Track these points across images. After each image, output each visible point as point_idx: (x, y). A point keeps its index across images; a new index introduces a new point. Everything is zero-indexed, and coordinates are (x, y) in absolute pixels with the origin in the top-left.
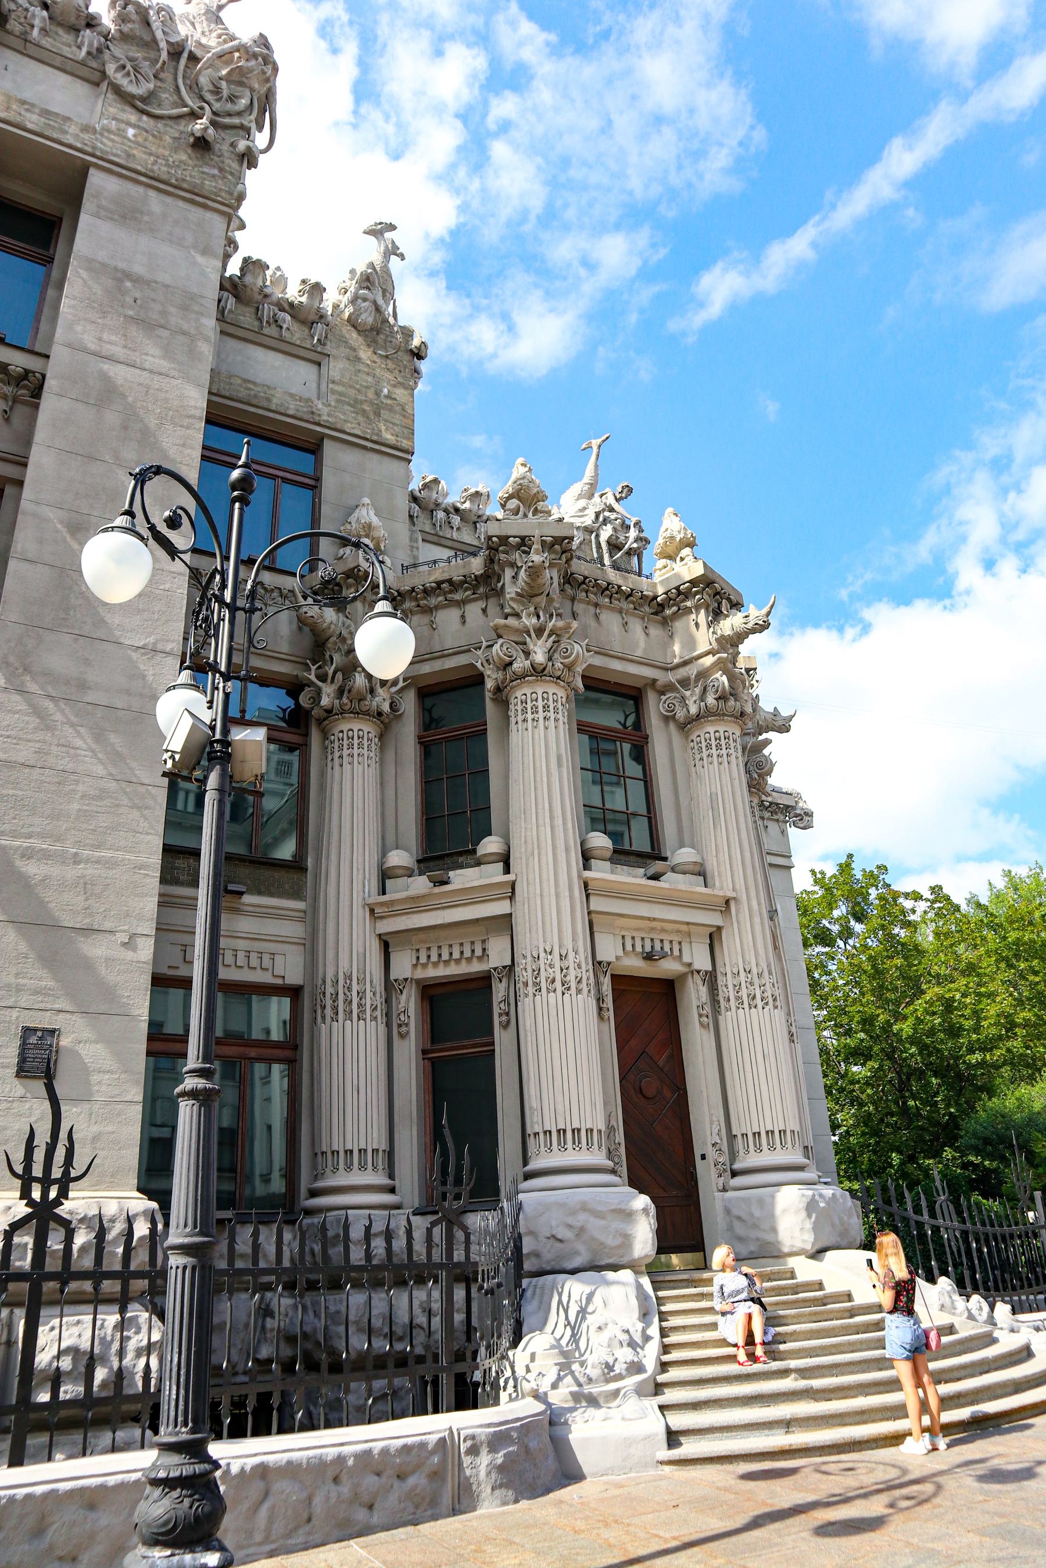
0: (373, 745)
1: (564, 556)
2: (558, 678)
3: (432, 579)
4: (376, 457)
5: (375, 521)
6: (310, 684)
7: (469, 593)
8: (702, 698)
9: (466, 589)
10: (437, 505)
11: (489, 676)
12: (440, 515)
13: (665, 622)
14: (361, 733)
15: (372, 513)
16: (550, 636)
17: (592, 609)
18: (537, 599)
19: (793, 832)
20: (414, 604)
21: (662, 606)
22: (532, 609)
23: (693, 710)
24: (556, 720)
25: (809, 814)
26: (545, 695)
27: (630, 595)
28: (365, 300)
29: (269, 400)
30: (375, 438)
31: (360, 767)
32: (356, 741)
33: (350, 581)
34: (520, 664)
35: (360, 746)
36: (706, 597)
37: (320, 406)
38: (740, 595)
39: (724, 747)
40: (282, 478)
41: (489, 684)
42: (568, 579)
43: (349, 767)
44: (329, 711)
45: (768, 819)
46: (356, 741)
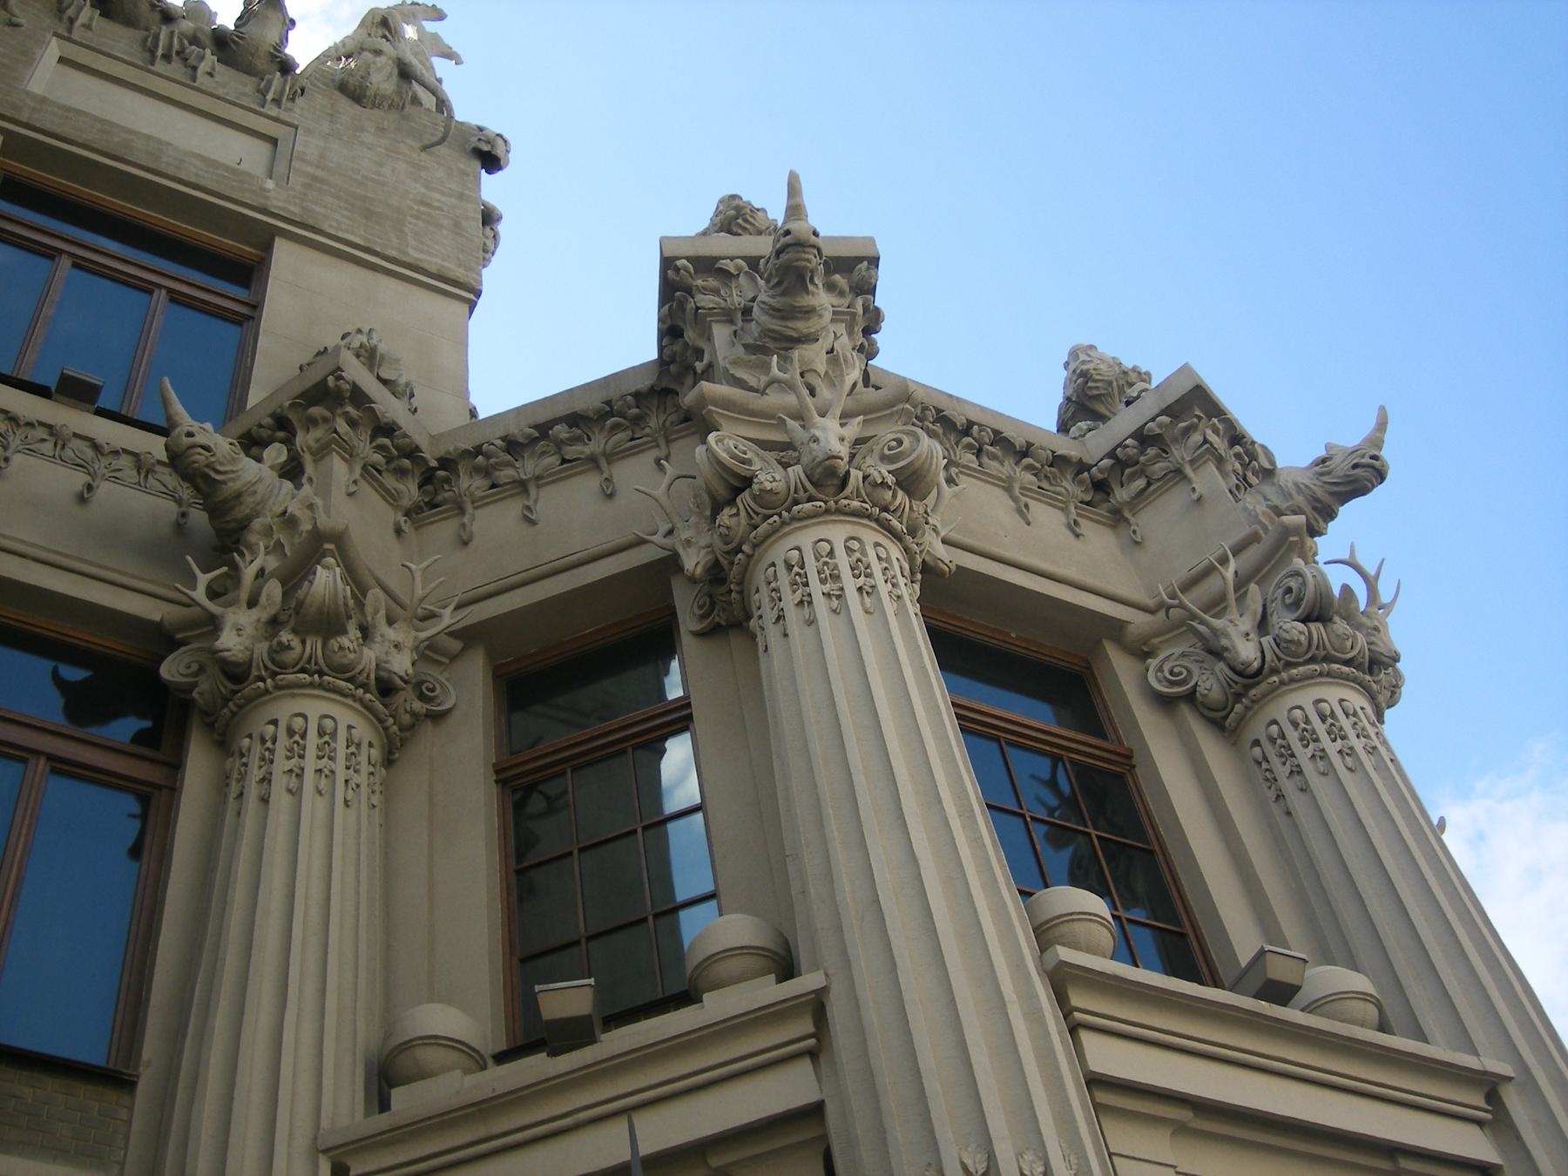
0: (363, 758)
9: (616, 428)
13: (1117, 519)
20: (479, 483)
27: (1025, 454)
28: (378, 53)
31: (321, 803)
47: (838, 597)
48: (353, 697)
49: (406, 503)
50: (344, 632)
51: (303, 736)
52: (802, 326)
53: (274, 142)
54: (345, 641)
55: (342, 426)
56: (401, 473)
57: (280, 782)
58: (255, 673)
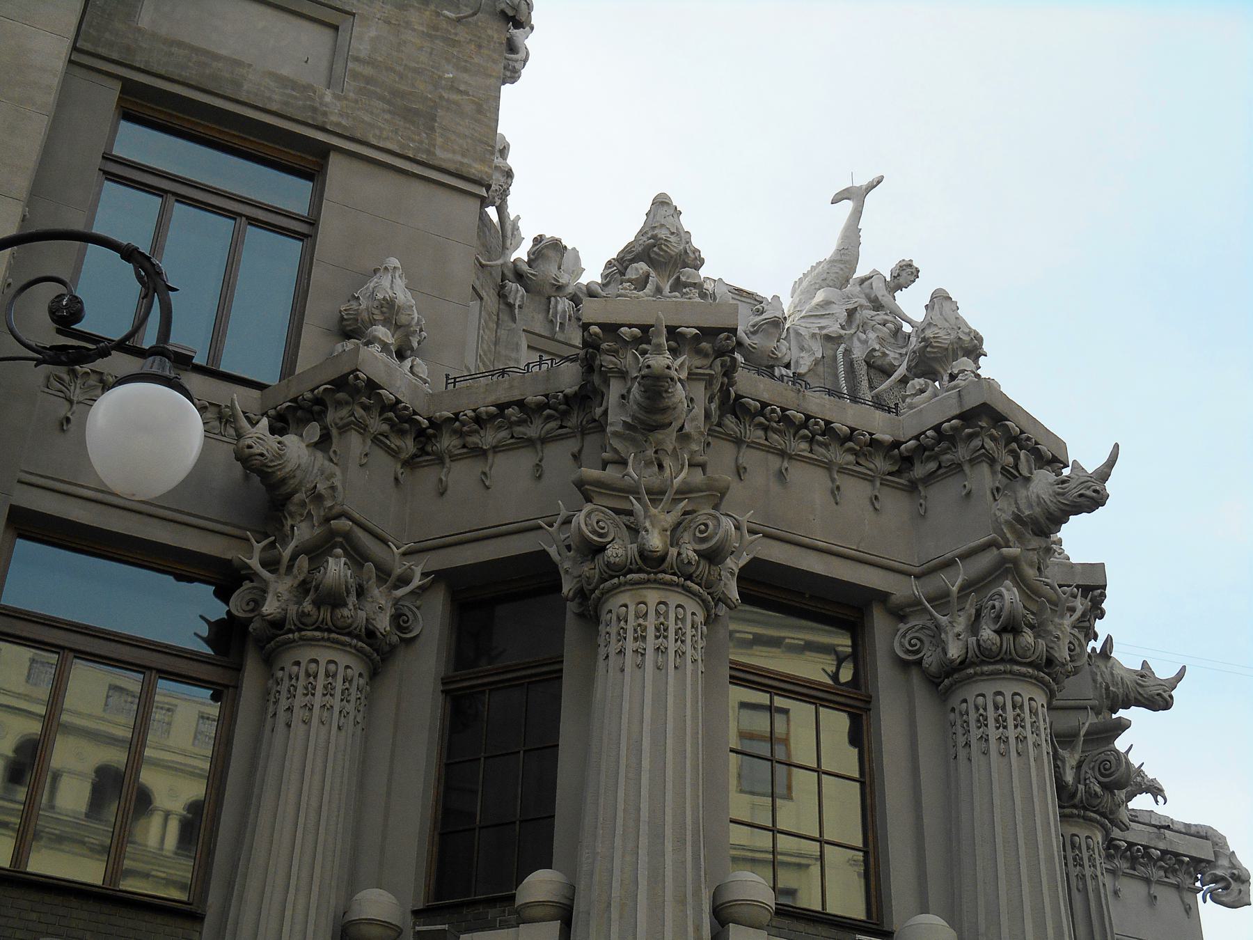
0: (353, 690)
1: (718, 362)
2: (689, 577)
3: (492, 398)
4: (419, 188)
5: (402, 295)
6: (252, 576)
7: (553, 424)
8: (974, 628)
9: (549, 418)
10: (560, 288)
11: (567, 572)
12: (564, 304)
13: (912, 488)
14: (332, 667)
15: (400, 283)
16: (676, 501)
17: (775, 462)
18: (659, 435)
19: (1209, 912)
20: (456, 442)
21: (907, 461)
22: (650, 452)
23: (954, 651)
24: (680, 654)
25: (1240, 878)
26: (662, 608)
29: (238, 85)
30: (422, 157)
31: (324, 730)
32: (321, 681)
33: (341, 396)
34: (617, 551)
35: (329, 691)
36: (989, 444)
37: (328, 98)
38: (1062, 445)
39: (1011, 723)
40: (248, 218)
41: (567, 587)
42: (733, 406)
43: (302, 727)
44: (278, 624)
45: (1159, 882)
46: (321, 681)
47: (643, 655)
48: (350, 645)
49: (404, 456)
50: (345, 605)
51: (315, 677)
52: (659, 418)
53: (336, 28)
54: (346, 612)
55: (359, 412)
56: (402, 433)
57: (298, 714)
58: (287, 626)
